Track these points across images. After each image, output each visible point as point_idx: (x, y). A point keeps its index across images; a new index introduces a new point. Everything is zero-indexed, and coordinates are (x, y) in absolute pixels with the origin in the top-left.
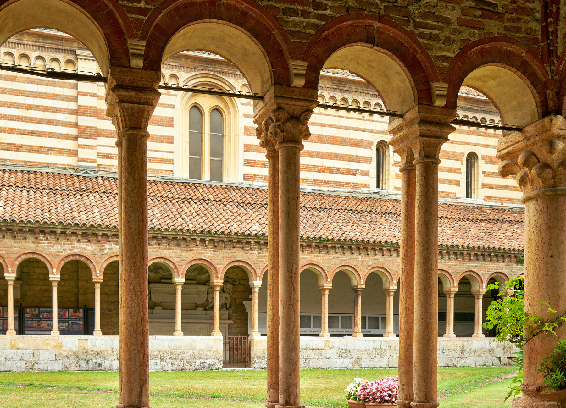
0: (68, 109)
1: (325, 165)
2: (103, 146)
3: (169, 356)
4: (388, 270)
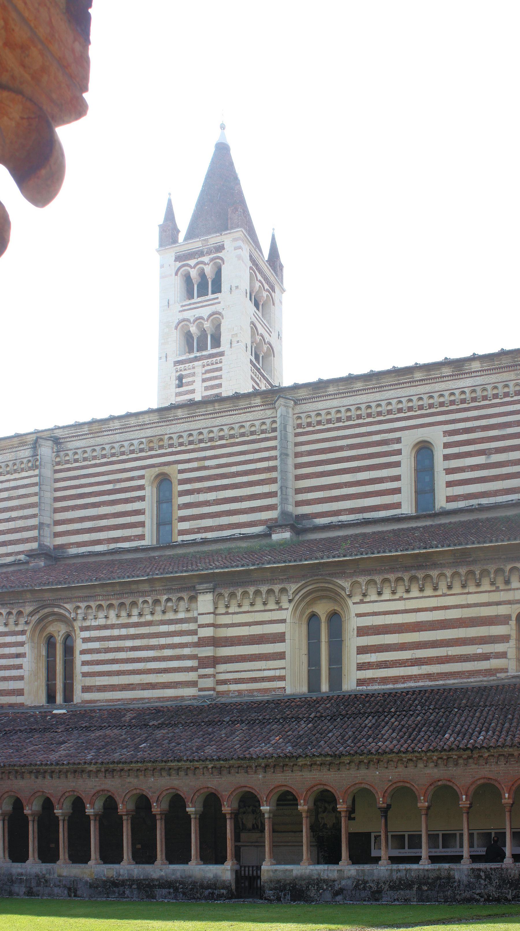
0: (193, 643)
1: (451, 654)
2: (221, 673)
3: (181, 886)
4: (413, 784)
